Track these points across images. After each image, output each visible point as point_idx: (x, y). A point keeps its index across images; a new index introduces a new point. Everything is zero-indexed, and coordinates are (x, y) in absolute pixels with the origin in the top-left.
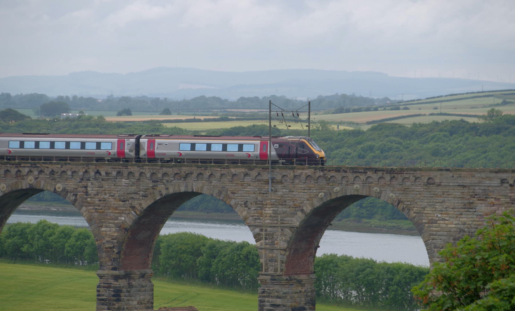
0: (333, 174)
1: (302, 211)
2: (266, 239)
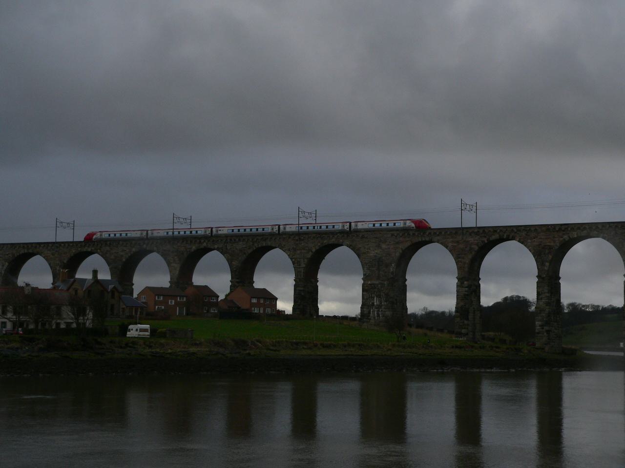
0: (324, 235)
1: (312, 251)
2: (297, 263)
